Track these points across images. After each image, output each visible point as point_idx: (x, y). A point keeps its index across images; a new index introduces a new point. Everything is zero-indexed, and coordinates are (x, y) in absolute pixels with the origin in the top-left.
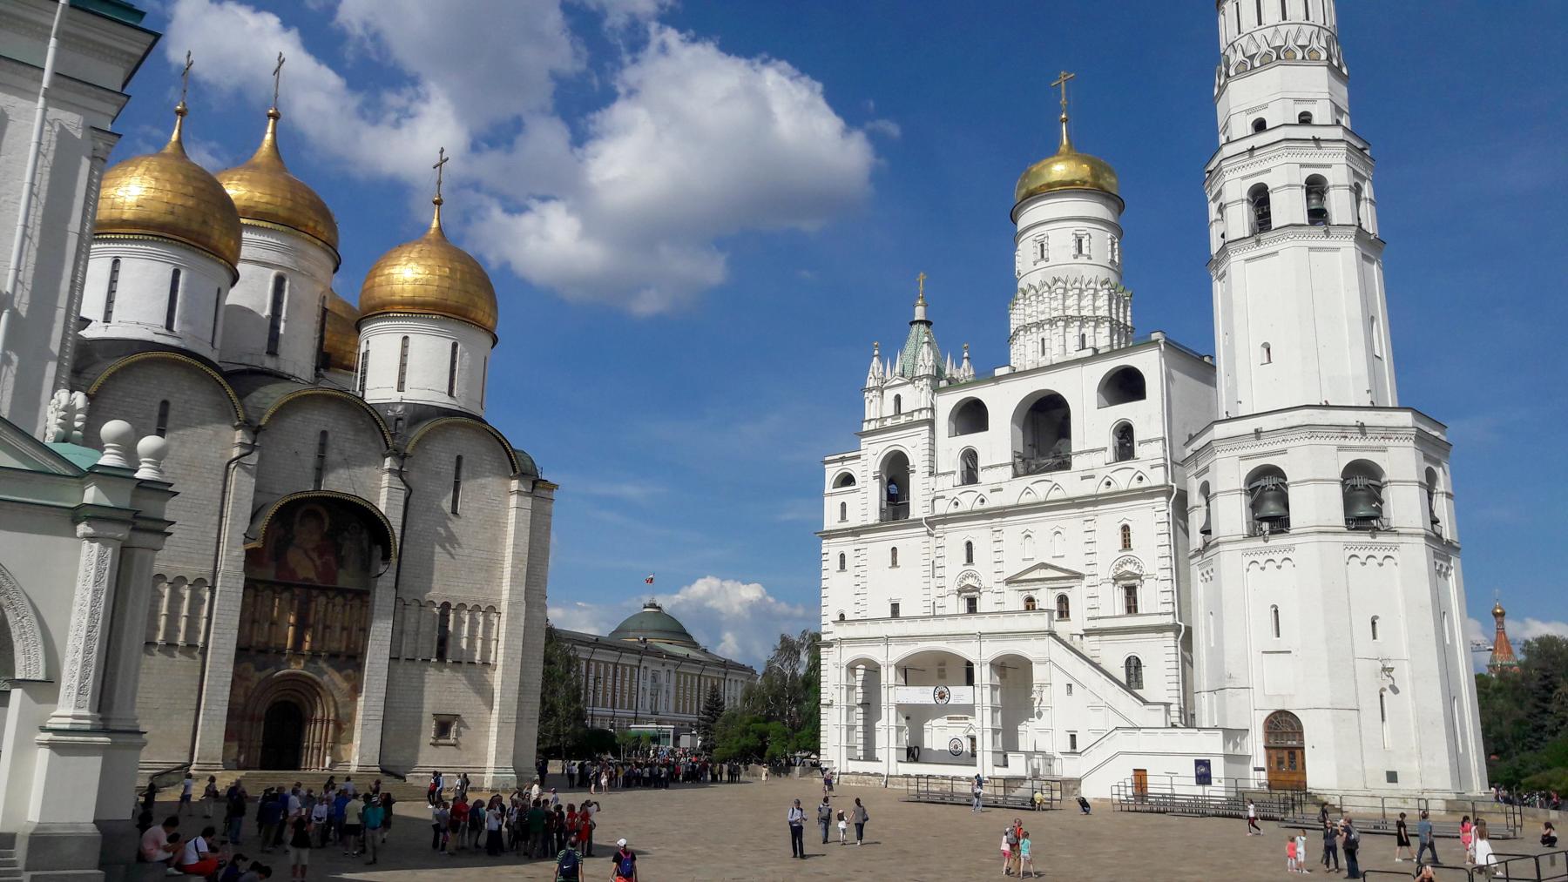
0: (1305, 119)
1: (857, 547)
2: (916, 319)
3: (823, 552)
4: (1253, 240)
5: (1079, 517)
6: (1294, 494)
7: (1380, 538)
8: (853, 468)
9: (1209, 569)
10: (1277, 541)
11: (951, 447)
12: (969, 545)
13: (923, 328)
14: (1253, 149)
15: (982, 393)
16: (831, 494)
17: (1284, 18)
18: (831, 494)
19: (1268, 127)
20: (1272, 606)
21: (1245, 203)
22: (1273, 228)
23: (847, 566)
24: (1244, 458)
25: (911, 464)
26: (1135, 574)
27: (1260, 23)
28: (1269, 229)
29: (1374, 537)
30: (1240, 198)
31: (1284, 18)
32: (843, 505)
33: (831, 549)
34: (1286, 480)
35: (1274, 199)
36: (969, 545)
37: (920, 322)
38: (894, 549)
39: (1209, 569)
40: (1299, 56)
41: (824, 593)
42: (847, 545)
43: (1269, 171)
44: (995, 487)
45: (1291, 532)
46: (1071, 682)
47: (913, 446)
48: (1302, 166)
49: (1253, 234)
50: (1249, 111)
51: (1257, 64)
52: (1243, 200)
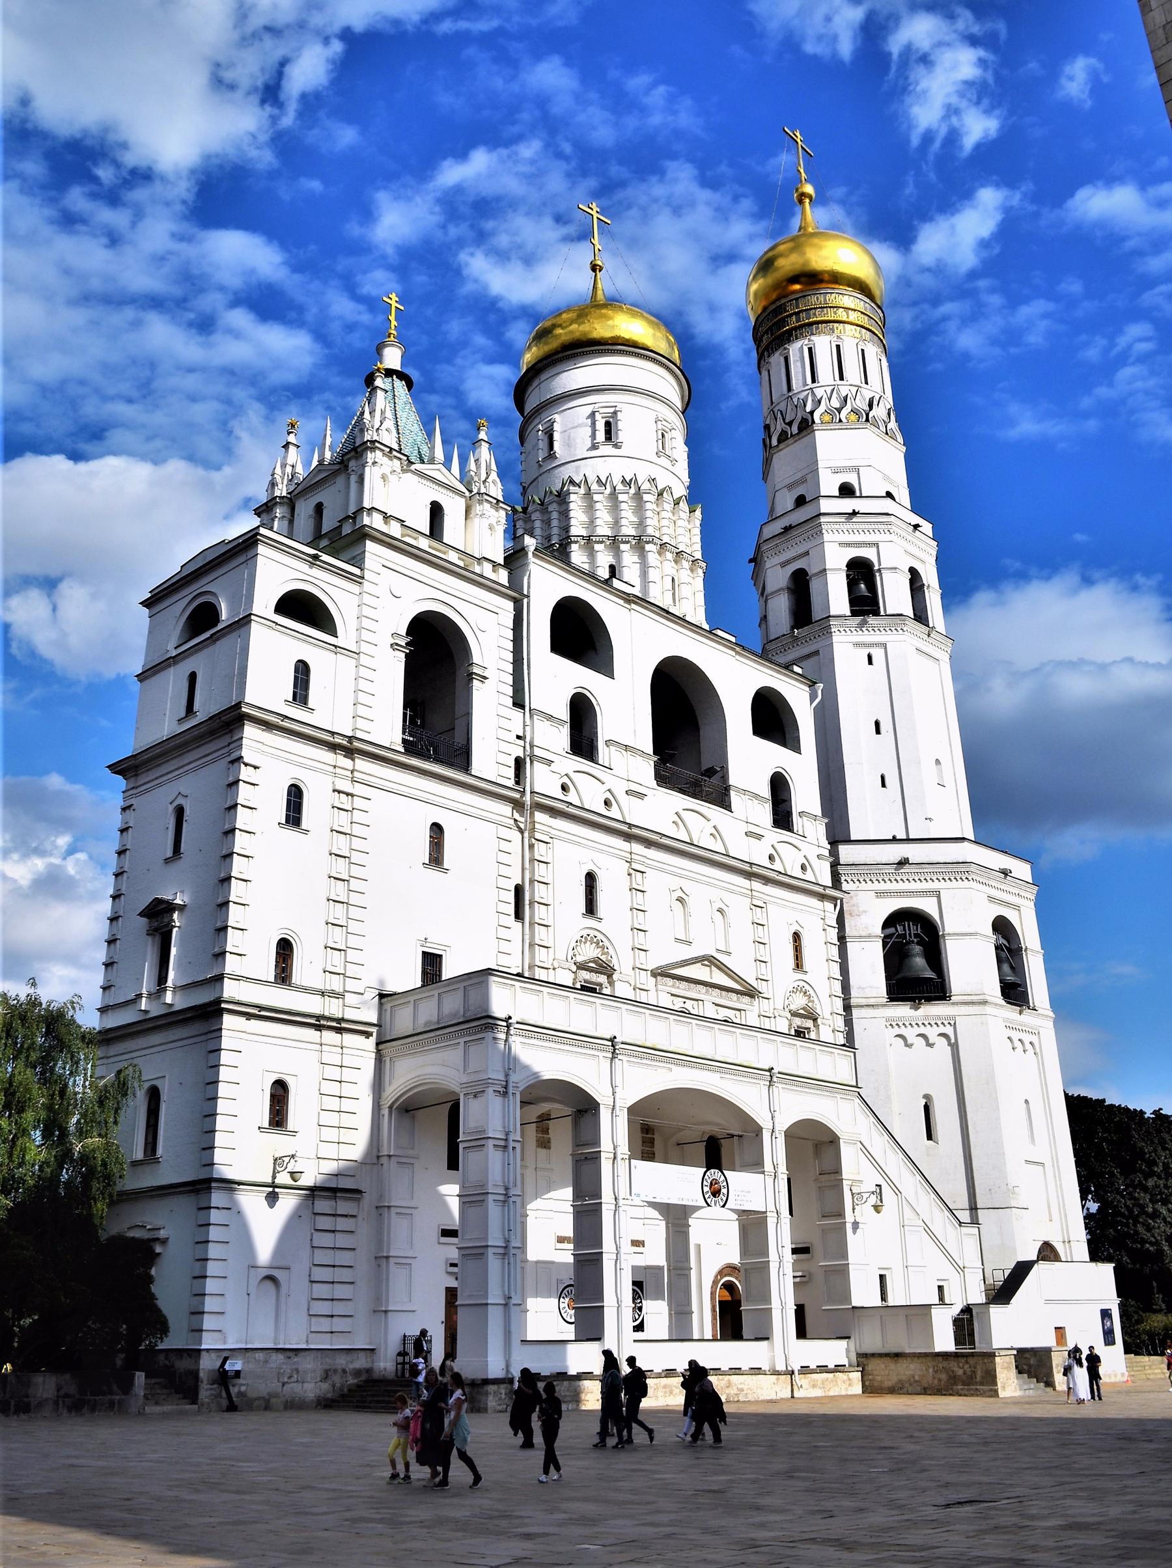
7: (1027, 1018)
14: (854, 513)
19: (858, 494)
22: (882, 613)
24: (880, 894)
28: (876, 613)
49: (854, 613)
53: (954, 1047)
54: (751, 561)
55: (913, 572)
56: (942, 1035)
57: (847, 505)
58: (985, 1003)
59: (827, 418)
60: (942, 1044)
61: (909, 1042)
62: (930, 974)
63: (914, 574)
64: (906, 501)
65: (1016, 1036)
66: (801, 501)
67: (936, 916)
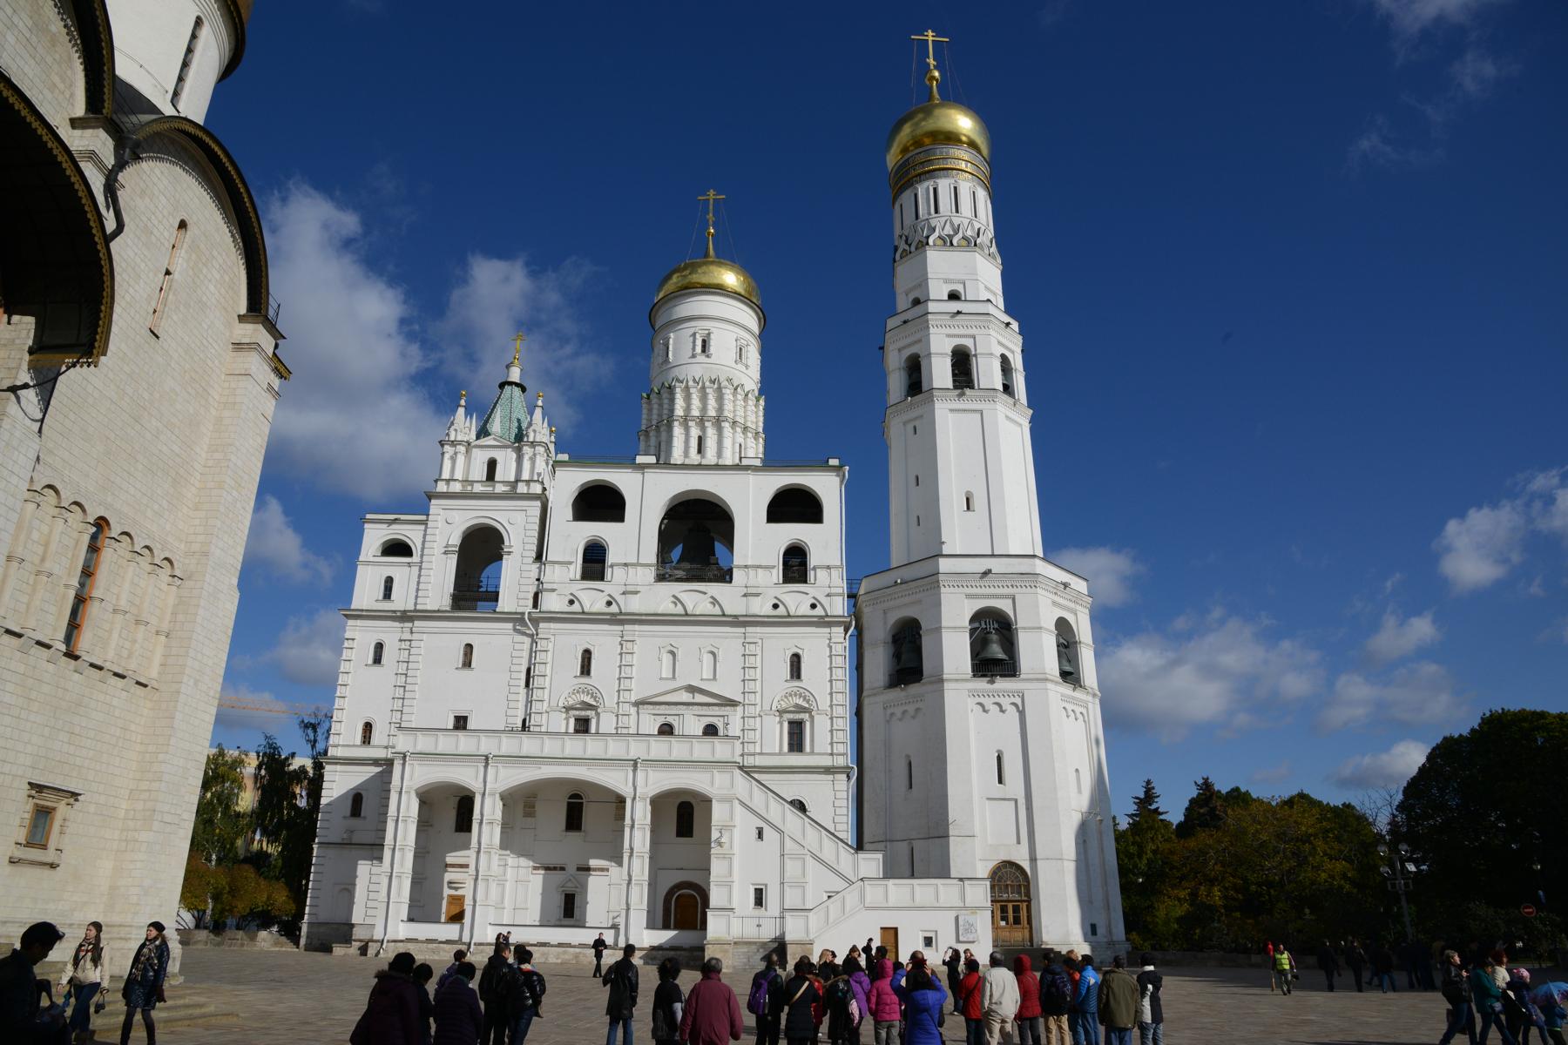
1: (407, 636)
2: (510, 380)
3: (347, 635)
5: (737, 637)
6: (1024, 642)
7: (1079, 694)
8: (410, 534)
9: (911, 709)
11: (569, 537)
12: (587, 654)
13: (517, 391)
15: (620, 478)
16: (368, 563)
17: (976, 217)
18: (368, 563)
22: (976, 387)
23: (384, 659)
24: (969, 596)
25: (507, 543)
26: (805, 708)
27: (957, 211)
29: (1074, 690)
31: (976, 217)
32: (389, 582)
33: (361, 636)
36: (587, 654)
37: (517, 385)
38: (469, 647)
39: (911, 709)
41: (340, 691)
42: (390, 633)
44: (630, 588)
46: (761, 824)
47: (516, 524)
48: (1000, 343)
49: (955, 387)
50: (946, 281)
52: (946, 354)
53: (1022, 713)
55: (1004, 357)
56: (1014, 704)
57: (954, 306)
58: (1047, 680)
59: (940, 242)
60: (1012, 713)
61: (987, 708)
62: (1001, 655)
63: (1004, 359)
64: (1001, 305)
65: (1070, 707)
67: (1011, 614)
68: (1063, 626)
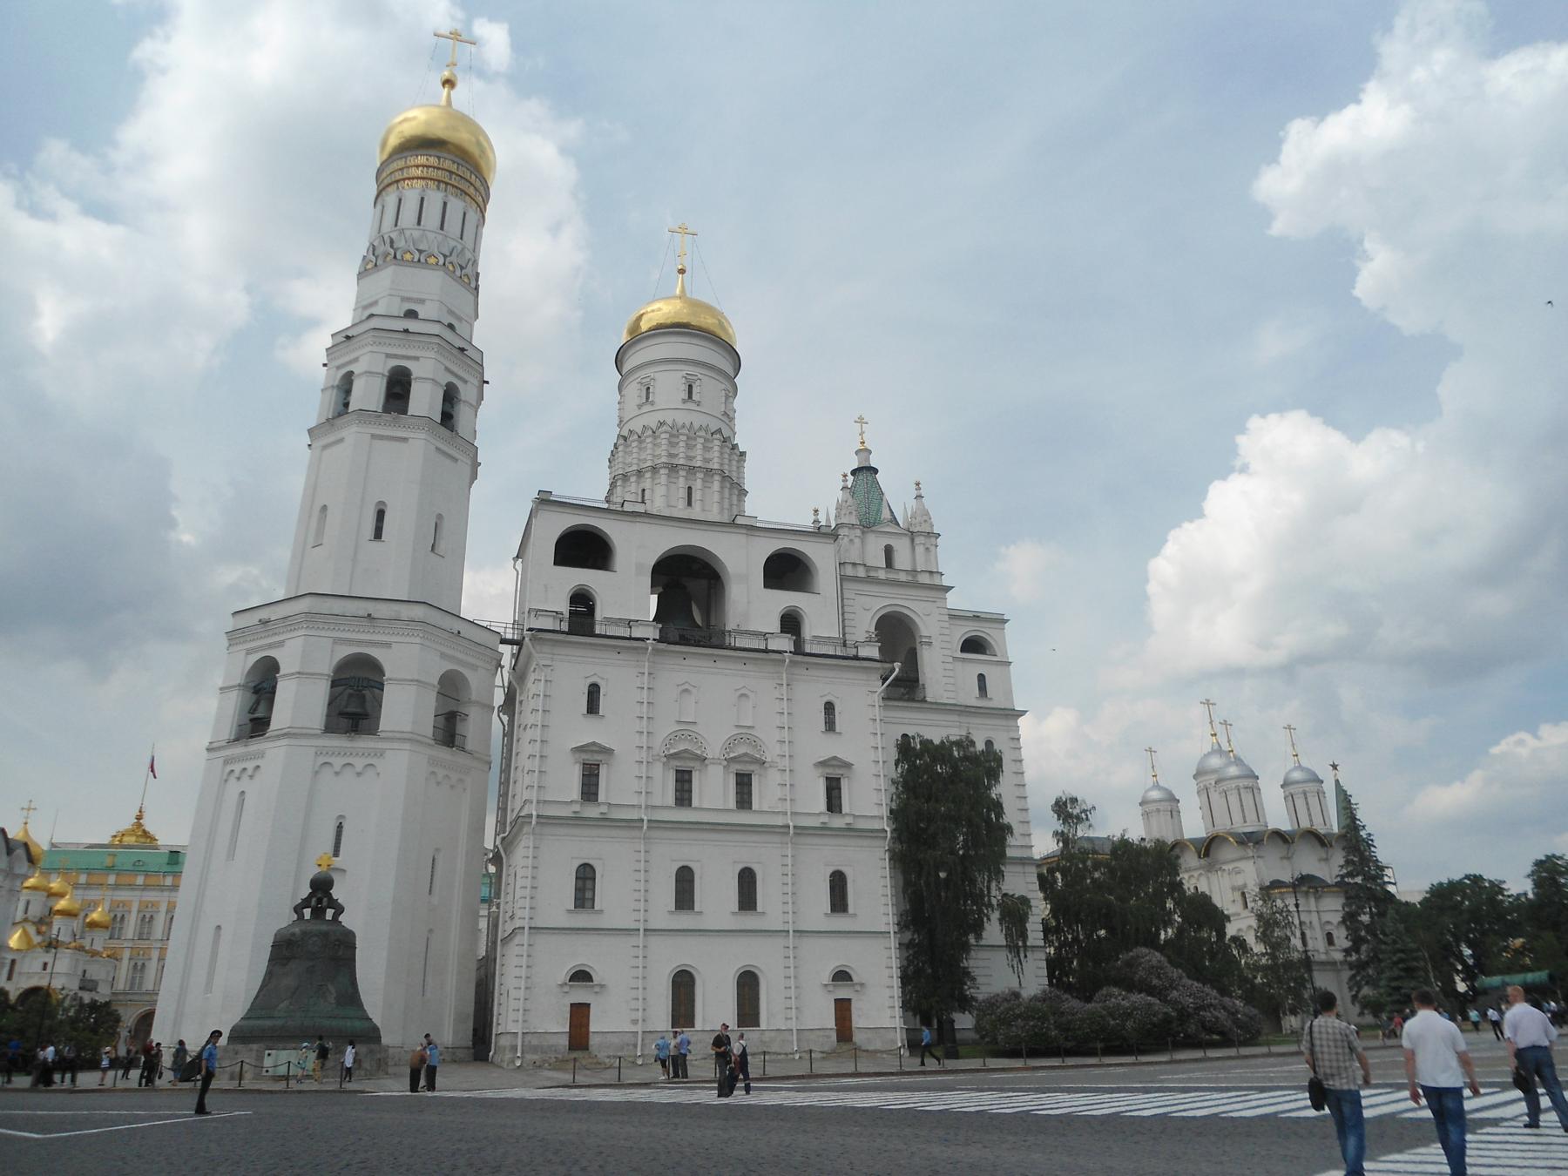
0: (451, 326)
4: (387, 417)
9: (250, 765)
10: (364, 743)
14: (406, 331)
19: (420, 317)
20: (341, 816)
21: (385, 381)
24: (337, 641)
28: (404, 412)
30: (381, 371)
34: (384, 676)
35: (415, 388)
40: (458, 273)
43: (417, 358)
45: (382, 735)
48: (447, 369)
50: (404, 299)
51: (422, 260)
52: (383, 375)
54: (325, 365)
66: (372, 316)
68: (451, 687)
